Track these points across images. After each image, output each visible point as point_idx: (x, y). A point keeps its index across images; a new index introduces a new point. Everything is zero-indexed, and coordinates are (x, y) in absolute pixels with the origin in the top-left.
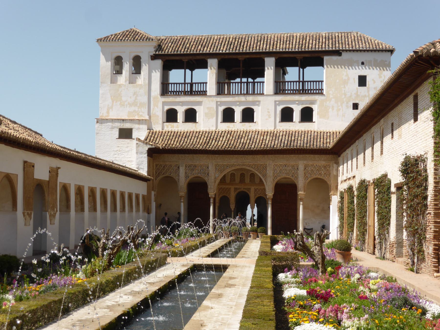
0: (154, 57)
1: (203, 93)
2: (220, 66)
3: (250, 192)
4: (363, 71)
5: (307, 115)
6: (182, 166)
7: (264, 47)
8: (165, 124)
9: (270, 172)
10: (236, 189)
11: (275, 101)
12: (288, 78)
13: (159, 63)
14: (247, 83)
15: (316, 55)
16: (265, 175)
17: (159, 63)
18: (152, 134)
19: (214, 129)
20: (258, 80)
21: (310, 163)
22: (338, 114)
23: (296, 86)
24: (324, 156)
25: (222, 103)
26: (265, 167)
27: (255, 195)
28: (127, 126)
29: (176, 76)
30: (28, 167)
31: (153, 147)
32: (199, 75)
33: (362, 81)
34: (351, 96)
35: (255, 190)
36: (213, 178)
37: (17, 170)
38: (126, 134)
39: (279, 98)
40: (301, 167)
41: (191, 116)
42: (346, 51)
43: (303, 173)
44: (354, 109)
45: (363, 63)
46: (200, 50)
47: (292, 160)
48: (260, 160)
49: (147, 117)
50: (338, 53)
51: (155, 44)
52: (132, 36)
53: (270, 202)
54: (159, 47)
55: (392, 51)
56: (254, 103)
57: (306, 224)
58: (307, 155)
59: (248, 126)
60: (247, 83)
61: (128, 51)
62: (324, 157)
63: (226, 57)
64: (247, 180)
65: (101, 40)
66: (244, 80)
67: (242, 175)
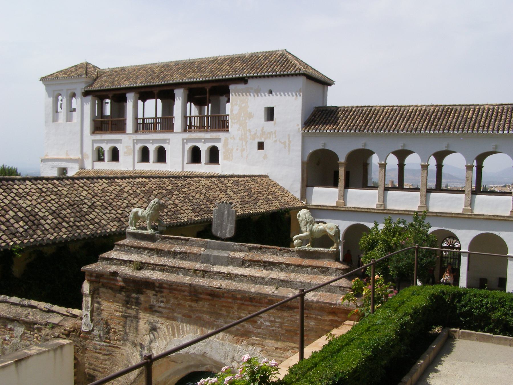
0: (86, 94)
4: (269, 101)
5: (214, 156)
8: (95, 163)
11: (183, 139)
13: (89, 98)
15: (223, 84)
19: (131, 169)
22: (242, 156)
25: (138, 141)
33: (270, 114)
34: (255, 134)
39: (187, 135)
42: (252, 77)
44: (259, 149)
49: (80, 156)
50: (244, 80)
56: (164, 141)
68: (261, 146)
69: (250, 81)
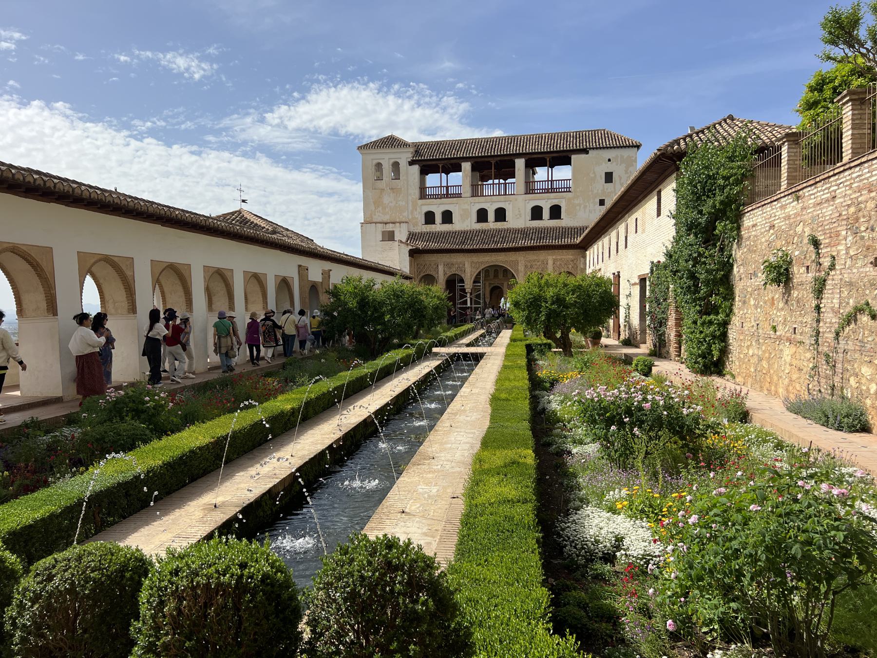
0: (412, 163)
1: (459, 196)
2: (474, 169)
7: (513, 150)
10: (490, 284)
12: (537, 177)
13: (416, 168)
14: (499, 184)
15: (564, 154)
16: (517, 271)
17: (416, 168)
18: (412, 236)
20: (509, 181)
23: (545, 186)
26: (516, 263)
28: (390, 227)
29: (433, 180)
30: (302, 270)
32: (455, 178)
33: (609, 178)
37: (292, 273)
38: (389, 236)
40: (550, 262)
41: (447, 217)
45: (609, 160)
46: (454, 154)
47: (542, 255)
50: (585, 151)
51: (412, 150)
52: (391, 142)
54: (417, 152)
55: (638, 147)
59: (500, 225)
60: (499, 184)
61: (386, 157)
62: (571, 252)
63: (479, 160)
64: (501, 275)
65: (361, 147)
66: (496, 181)
67: (496, 272)
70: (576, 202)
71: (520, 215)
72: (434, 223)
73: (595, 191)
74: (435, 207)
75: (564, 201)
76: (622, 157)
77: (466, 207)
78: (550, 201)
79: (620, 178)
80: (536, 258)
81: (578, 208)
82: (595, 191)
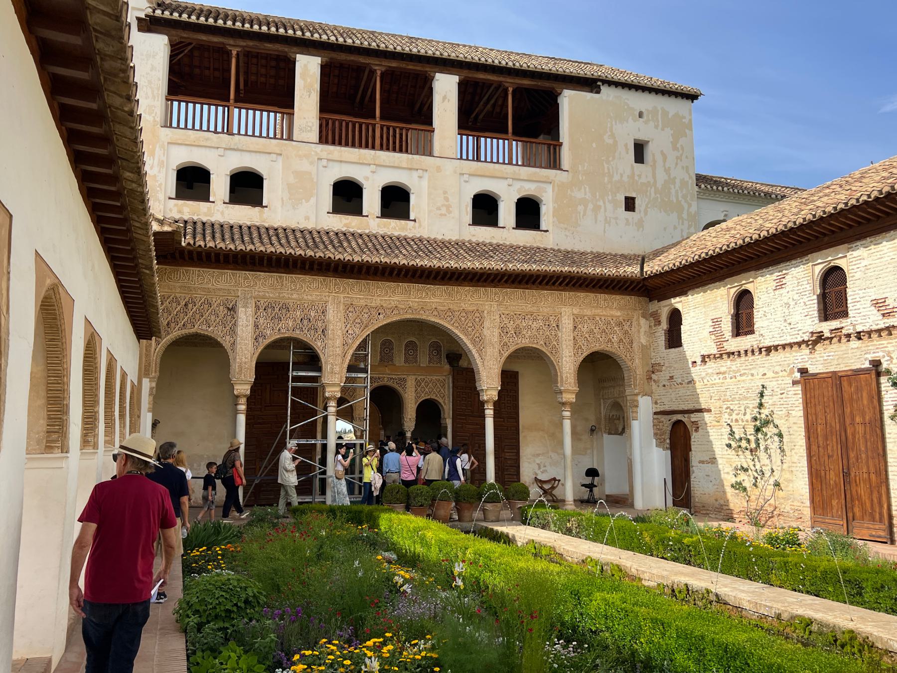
3: (404, 388)
6: (245, 306)
9: (491, 332)
15: (547, 84)
16: (479, 341)
21: (588, 312)
24: (618, 297)
27: (417, 397)
31: (167, 228)
35: (418, 383)
36: (338, 342)
40: (567, 323)
43: (572, 338)
48: (466, 299)
53: (489, 412)
57: (540, 468)
58: (579, 294)
59: (394, 227)
62: (618, 300)
68: (630, 204)
69: (604, 89)
70: (578, 195)
71: (448, 207)
72: (204, 196)
73: (616, 178)
74: (214, 153)
75: (549, 188)
76: (665, 113)
77: (305, 166)
78: (518, 185)
79: (665, 158)
80: (529, 308)
81: (581, 208)
82: (616, 178)
